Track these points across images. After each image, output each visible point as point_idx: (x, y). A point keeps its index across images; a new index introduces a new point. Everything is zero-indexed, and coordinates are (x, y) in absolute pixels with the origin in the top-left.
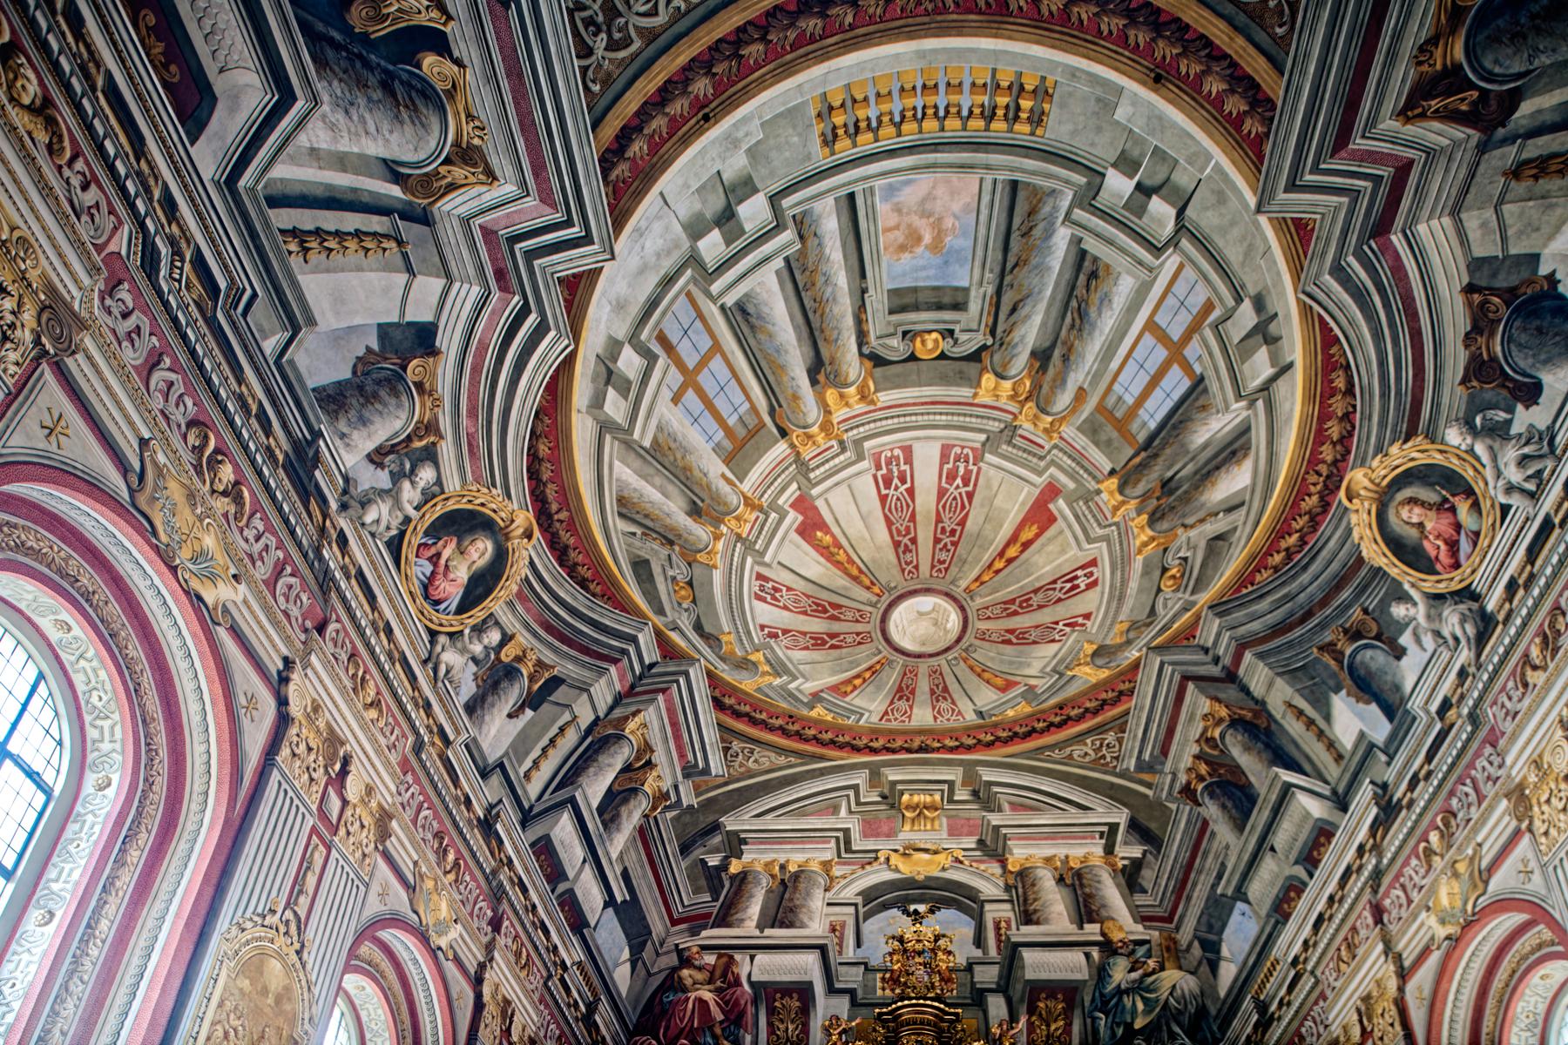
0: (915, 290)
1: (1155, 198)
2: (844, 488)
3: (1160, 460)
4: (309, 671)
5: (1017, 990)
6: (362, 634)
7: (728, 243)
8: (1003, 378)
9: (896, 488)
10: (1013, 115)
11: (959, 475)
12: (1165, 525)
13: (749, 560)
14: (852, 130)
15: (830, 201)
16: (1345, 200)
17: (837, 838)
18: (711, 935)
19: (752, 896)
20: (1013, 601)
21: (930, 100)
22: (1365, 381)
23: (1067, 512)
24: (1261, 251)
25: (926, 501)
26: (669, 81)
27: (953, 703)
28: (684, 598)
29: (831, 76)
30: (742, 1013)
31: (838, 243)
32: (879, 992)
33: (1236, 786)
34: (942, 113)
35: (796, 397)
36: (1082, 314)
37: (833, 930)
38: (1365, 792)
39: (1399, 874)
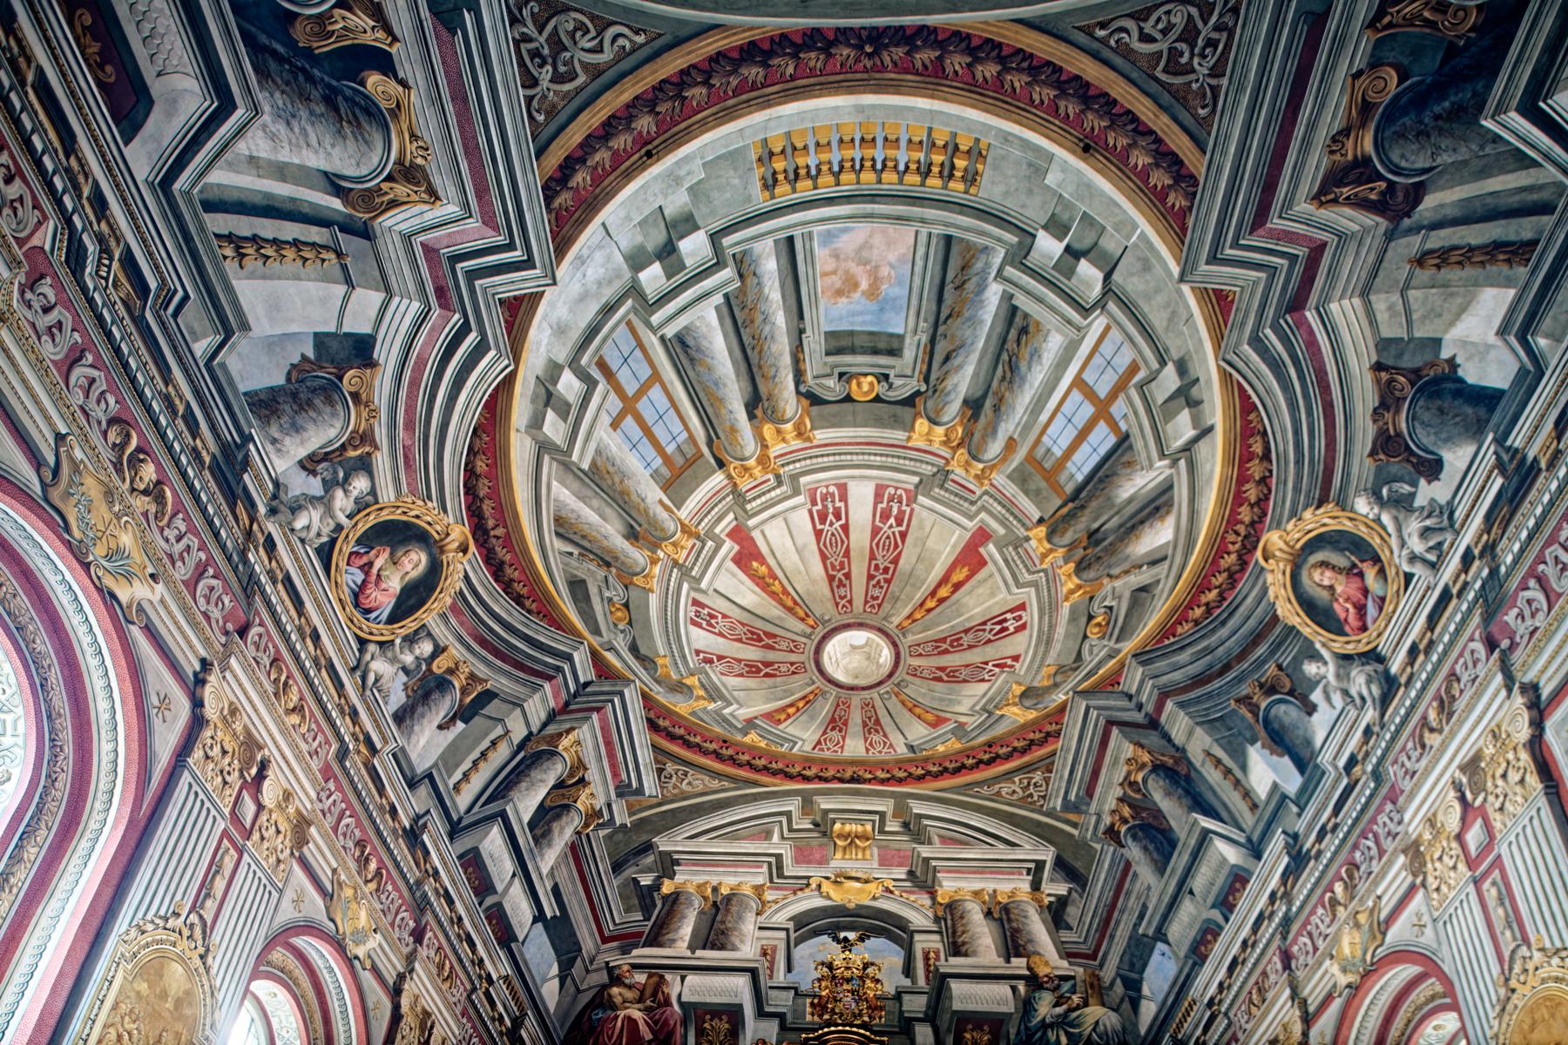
0: (851, 333)
1: (1083, 261)
2: (779, 522)
3: (1087, 511)
4: (228, 674)
5: (944, 1020)
6: (287, 640)
7: (669, 277)
8: (936, 423)
9: (831, 524)
10: (948, 173)
11: (893, 515)
12: (1091, 574)
13: (685, 586)
14: (792, 176)
15: (769, 242)
16: (1263, 275)
17: (770, 864)
18: (642, 954)
19: (684, 917)
20: (943, 640)
21: (869, 153)
22: (1281, 448)
23: (997, 556)
24: (1184, 317)
25: (860, 538)
26: (613, 116)
27: (885, 735)
28: (620, 620)
29: (772, 124)
30: (672, 1033)
31: (777, 284)
32: (809, 1018)
33: (1158, 830)
34: (879, 166)
35: (733, 430)
36: (1013, 367)
37: (765, 954)
38: (1277, 842)
39: (1307, 922)
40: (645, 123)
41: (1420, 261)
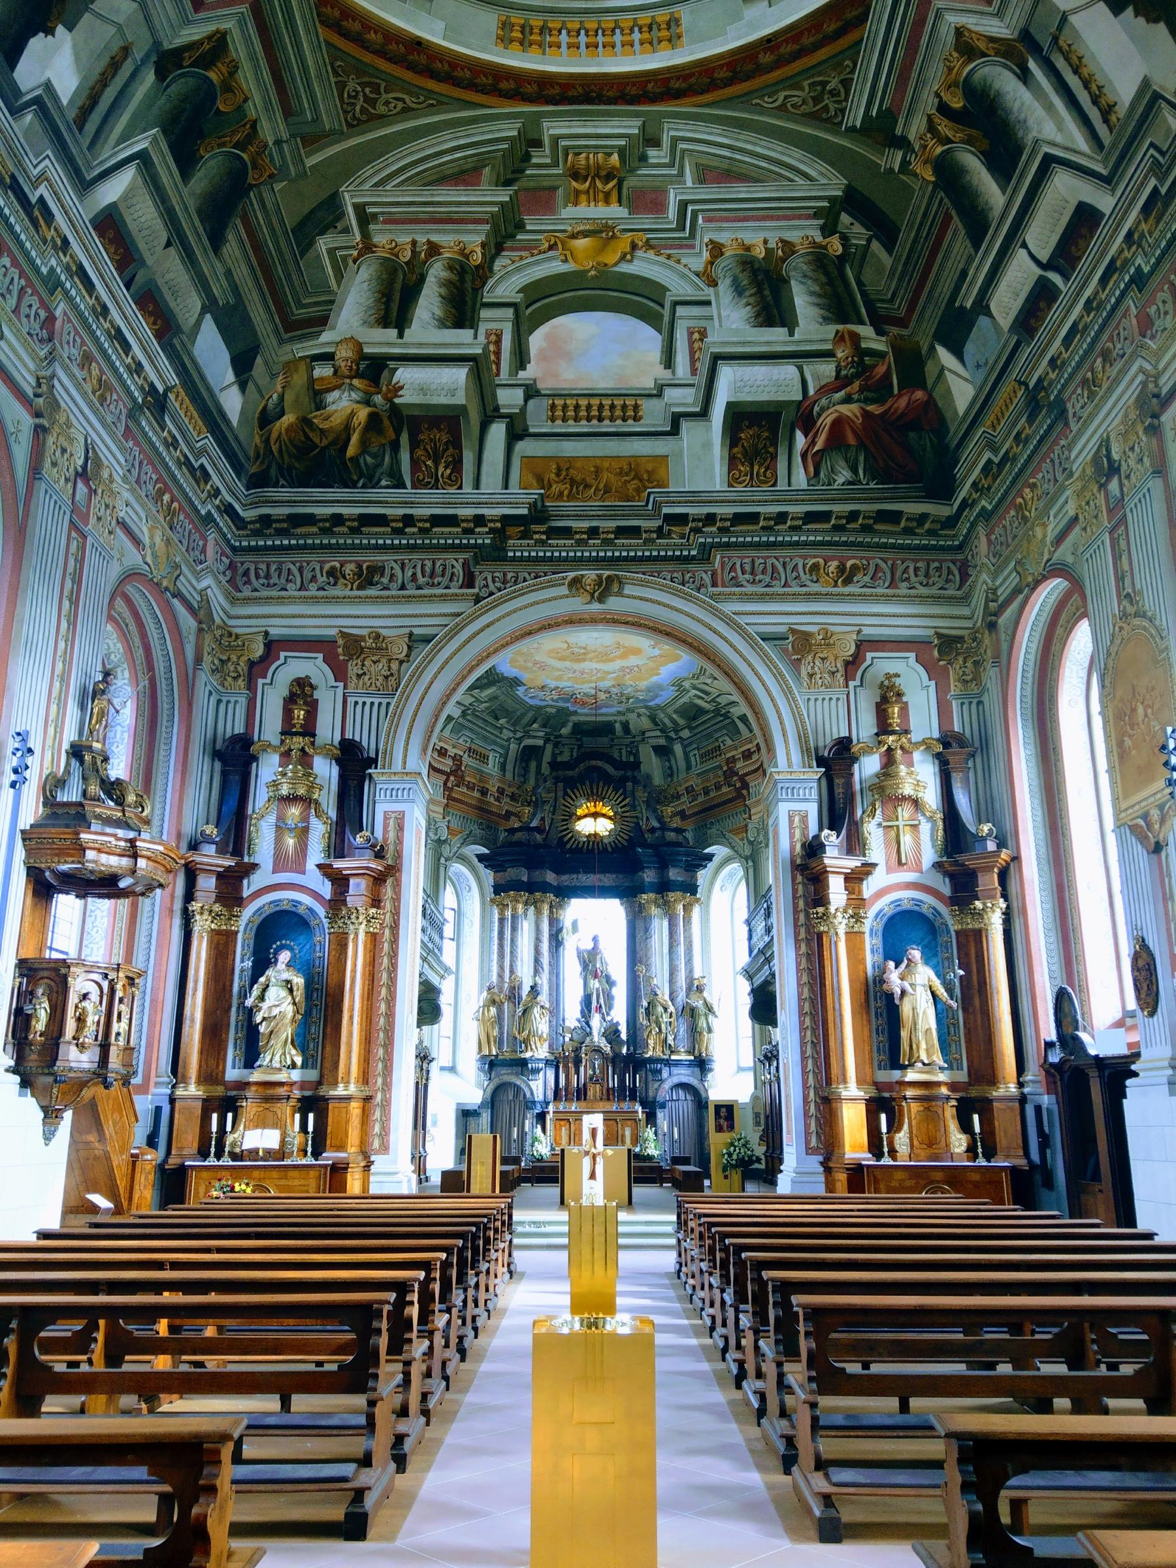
40: (766, 59)
41: (126, 51)
